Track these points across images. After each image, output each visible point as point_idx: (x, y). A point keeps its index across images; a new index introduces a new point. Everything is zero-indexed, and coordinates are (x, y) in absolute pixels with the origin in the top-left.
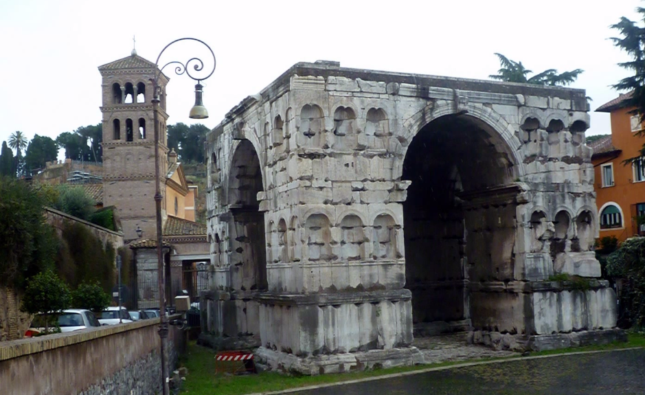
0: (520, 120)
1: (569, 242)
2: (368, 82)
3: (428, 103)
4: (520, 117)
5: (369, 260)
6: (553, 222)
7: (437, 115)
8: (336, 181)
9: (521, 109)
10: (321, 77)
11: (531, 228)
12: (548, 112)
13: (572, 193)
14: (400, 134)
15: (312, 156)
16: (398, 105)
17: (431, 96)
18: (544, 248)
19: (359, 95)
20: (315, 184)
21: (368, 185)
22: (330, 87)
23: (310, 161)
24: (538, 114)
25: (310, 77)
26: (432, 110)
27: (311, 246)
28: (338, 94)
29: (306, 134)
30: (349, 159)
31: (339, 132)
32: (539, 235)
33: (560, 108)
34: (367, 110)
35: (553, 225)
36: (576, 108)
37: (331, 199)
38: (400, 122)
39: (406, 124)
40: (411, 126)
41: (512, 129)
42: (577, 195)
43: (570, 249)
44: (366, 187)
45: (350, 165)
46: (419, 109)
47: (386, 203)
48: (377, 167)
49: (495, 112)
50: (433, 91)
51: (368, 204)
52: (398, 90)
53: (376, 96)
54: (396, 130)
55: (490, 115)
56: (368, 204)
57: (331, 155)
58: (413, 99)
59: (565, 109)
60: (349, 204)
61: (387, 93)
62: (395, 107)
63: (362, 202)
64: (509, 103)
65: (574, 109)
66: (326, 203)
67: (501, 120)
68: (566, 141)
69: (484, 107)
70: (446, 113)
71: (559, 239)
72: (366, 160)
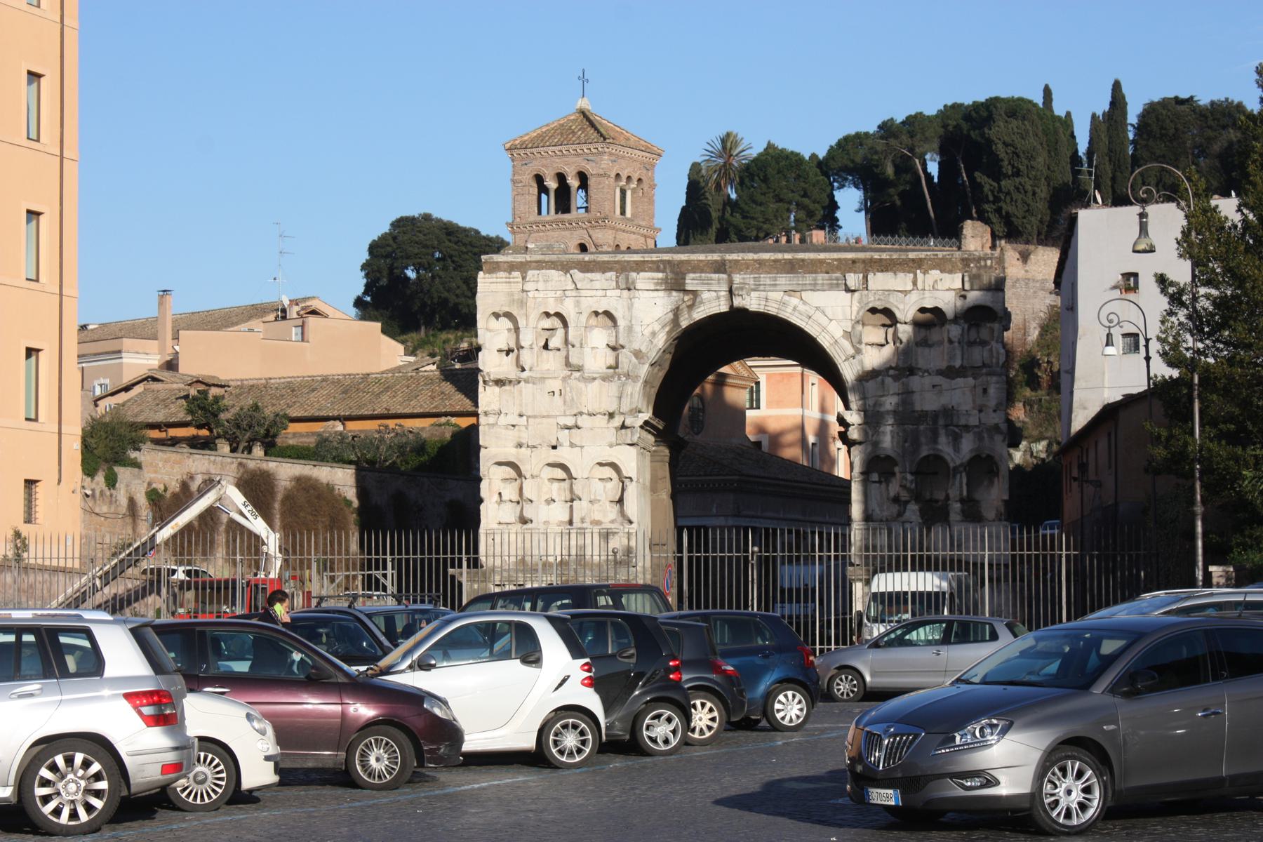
0: (854, 313)
1: (956, 506)
2: (589, 275)
3: (686, 298)
4: (855, 308)
5: (580, 525)
6: (911, 473)
7: (699, 314)
8: (535, 417)
9: (856, 294)
10: (516, 274)
11: (880, 482)
12: (914, 297)
13: (957, 426)
14: (636, 346)
15: (499, 383)
16: (636, 305)
17: (689, 288)
18: (907, 514)
19: (574, 293)
20: (503, 420)
21: (583, 421)
22: (528, 286)
23: (496, 389)
24: (891, 300)
25: (502, 274)
26: (691, 307)
27: (503, 505)
28: (541, 294)
29: (500, 351)
30: (556, 385)
31: (551, 345)
32: (892, 494)
33: (940, 287)
34: (583, 318)
35: (909, 477)
36: (972, 285)
37: (524, 441)
38: (637, 328)
39: (647, 332)
40: (654, 334)
41: (836, 330)
42: (967, 428)
43: (959, 518)
44: (579, 424)
45: (557, 393)
46: (669, 308)
47: (611, 446)
48: (599, 396)
49: (805, 303)
50: (691, 282)
51: (582, 447)
52: (633, 283)
53: (601, 293)
54: (630, 342)
55: (795, 309)
56: (582, 447)
57: (527, 381)
58: (661, 294)
59: (949, 289)
60: (554, 447)
61: (618, 287)
62: (630, 307)
63: (572, 445)
64: (832, 287)
65: (967, 286)
66: (520, 445)
67: (818, 316)
68: (951, 342)
69: (786, 298)
70: (716, 310)
71: (937, 501)
72: (582, 385)
